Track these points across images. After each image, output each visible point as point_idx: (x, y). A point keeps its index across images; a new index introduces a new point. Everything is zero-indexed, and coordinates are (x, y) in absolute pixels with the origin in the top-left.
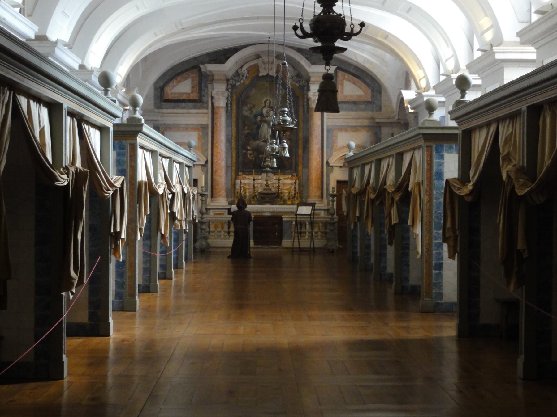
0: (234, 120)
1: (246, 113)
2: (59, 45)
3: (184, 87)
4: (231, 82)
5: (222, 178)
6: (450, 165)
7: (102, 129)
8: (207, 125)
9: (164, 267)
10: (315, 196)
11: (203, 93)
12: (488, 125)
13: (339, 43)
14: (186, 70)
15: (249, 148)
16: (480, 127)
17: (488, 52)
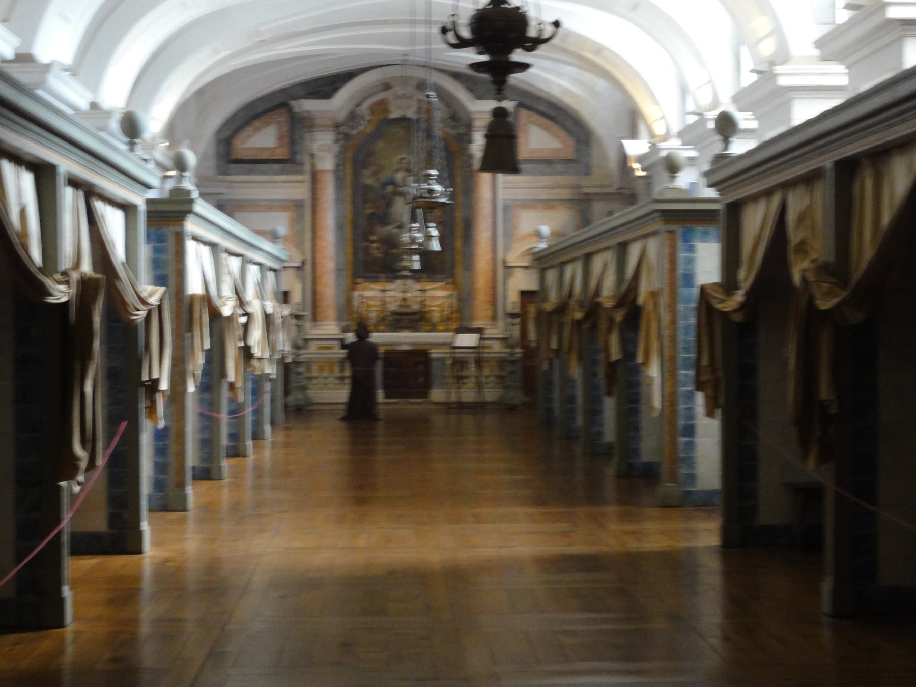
0: (348, 191)
1: (368, 179)
2: (55, 70)
3: (264, 139)
5: (330, 288)
6: (706, 262)
7: (127, 208)
9: (235, 436)
12: (768, 193)
13: (518, 56)
15: (374, 238)
16: (755, 198)
17: (766, 74)
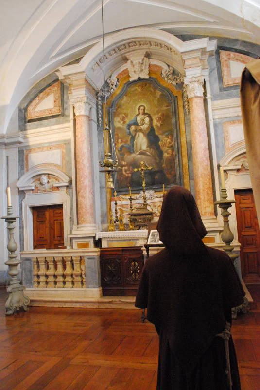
3: (47, 104)
4: (100, 94)
8: (70, 140)
14: (49, 85)
15: (124, 163)
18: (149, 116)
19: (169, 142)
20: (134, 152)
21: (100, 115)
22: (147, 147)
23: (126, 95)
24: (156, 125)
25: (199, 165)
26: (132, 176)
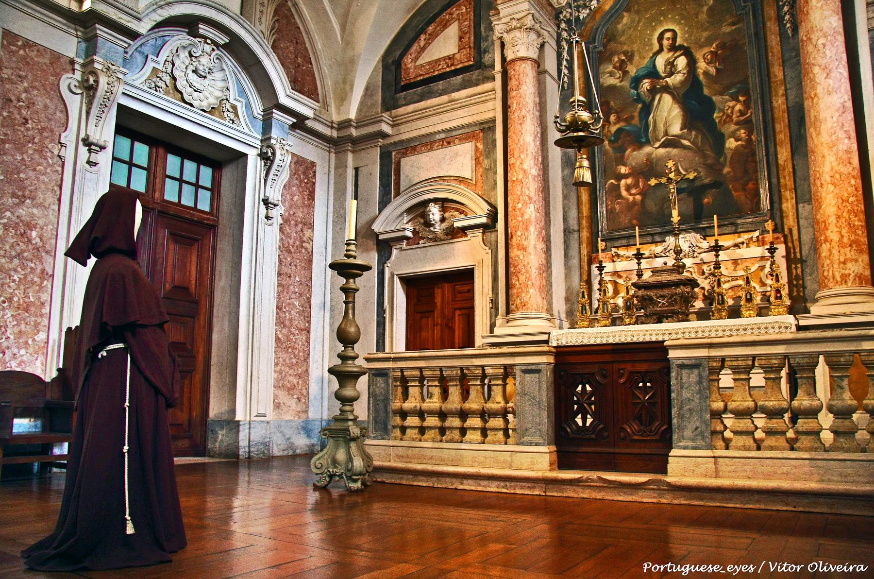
4: (565, 14)
10: (844, 278)
11: (484, 45)
15: (623, 170)
18: (687, 53)
19: (740, 111)
20: (648, 143)
21: (565, 63)
22: (681, 130)
23: (628, 10)
24: (706, 73)
25: (826, 152)
26: (642, 200)
